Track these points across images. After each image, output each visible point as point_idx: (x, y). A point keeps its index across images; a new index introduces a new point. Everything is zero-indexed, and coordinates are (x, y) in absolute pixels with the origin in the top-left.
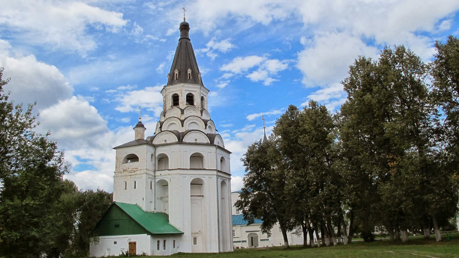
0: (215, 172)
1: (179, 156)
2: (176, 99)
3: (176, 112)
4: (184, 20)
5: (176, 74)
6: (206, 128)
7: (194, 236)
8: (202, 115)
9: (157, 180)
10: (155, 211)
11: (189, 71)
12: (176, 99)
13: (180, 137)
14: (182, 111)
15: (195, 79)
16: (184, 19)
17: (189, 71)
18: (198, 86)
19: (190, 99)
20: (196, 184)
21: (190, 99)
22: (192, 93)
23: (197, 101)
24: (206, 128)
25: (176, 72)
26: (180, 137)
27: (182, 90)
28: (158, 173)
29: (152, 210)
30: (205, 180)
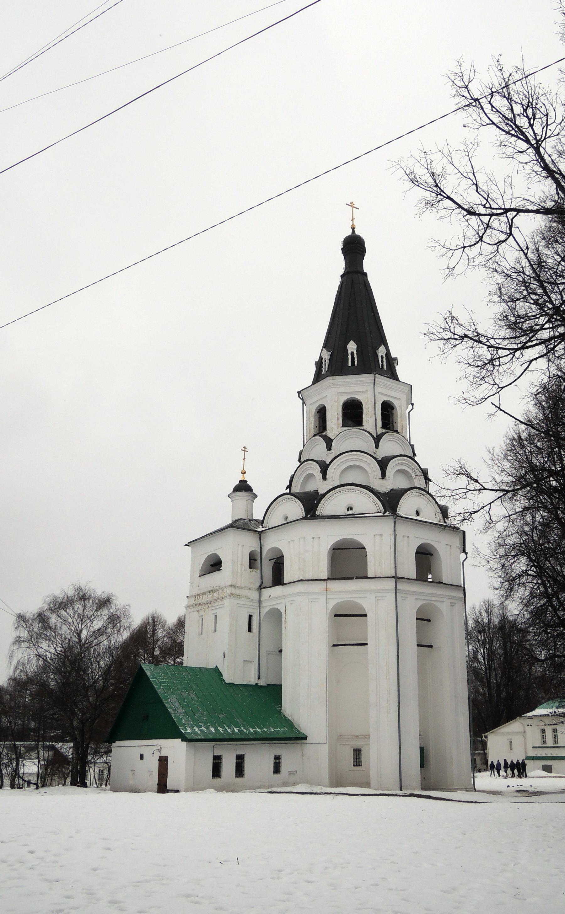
0: (391, 584)
1: (306, 548)
4: (353, 232)
6: (383, 476)
7: (357, 744)
8: (377, 447)
9: (264, 611)
10: (262, 683)
11: (352, 347)
13: (311, 503)
14: (329, 442)
16: (353, 229)
17: (352, 347)
19: (353, 413)
21: (353, 413)
24: (383, 476)
26: (311, 503)
27: (337, 392)
28: (266, 593)
29: (252, 680)
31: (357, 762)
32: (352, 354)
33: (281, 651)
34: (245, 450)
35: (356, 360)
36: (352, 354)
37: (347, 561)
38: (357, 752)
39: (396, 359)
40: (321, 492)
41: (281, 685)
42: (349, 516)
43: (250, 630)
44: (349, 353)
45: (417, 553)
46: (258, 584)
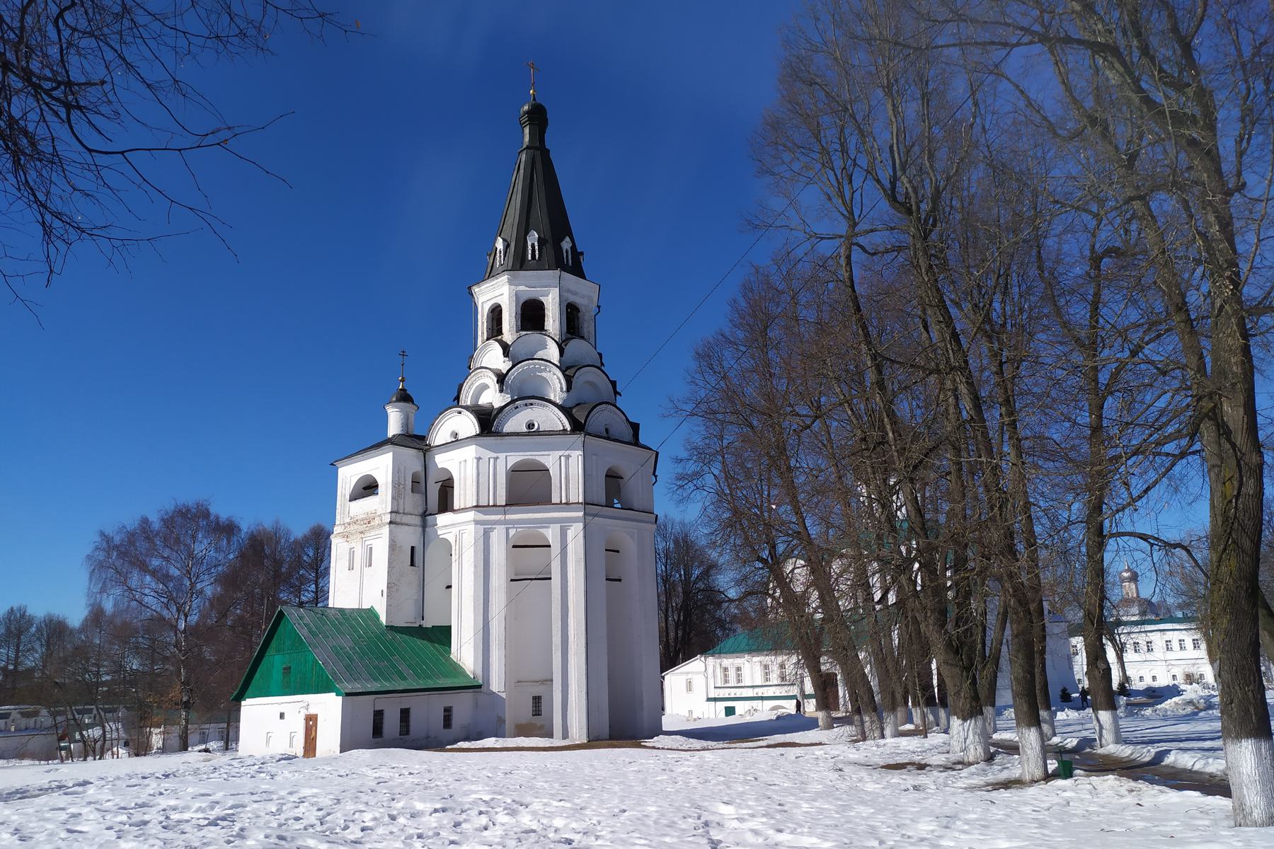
7: (537, 690)
19: (531, 315)
30: (551, 534)
31: (537, 712)
32: (533, 245)
33: (449, 587)
34: (403, 354)
36: (533, 245)
37: (528, 488)
38: (537, 700)
39: (582, 253)
40: (497, 405)
41: (450, 627)
43: (412, 564)
44: (529, 243)
45: (607, 476)
46: (421, 510)
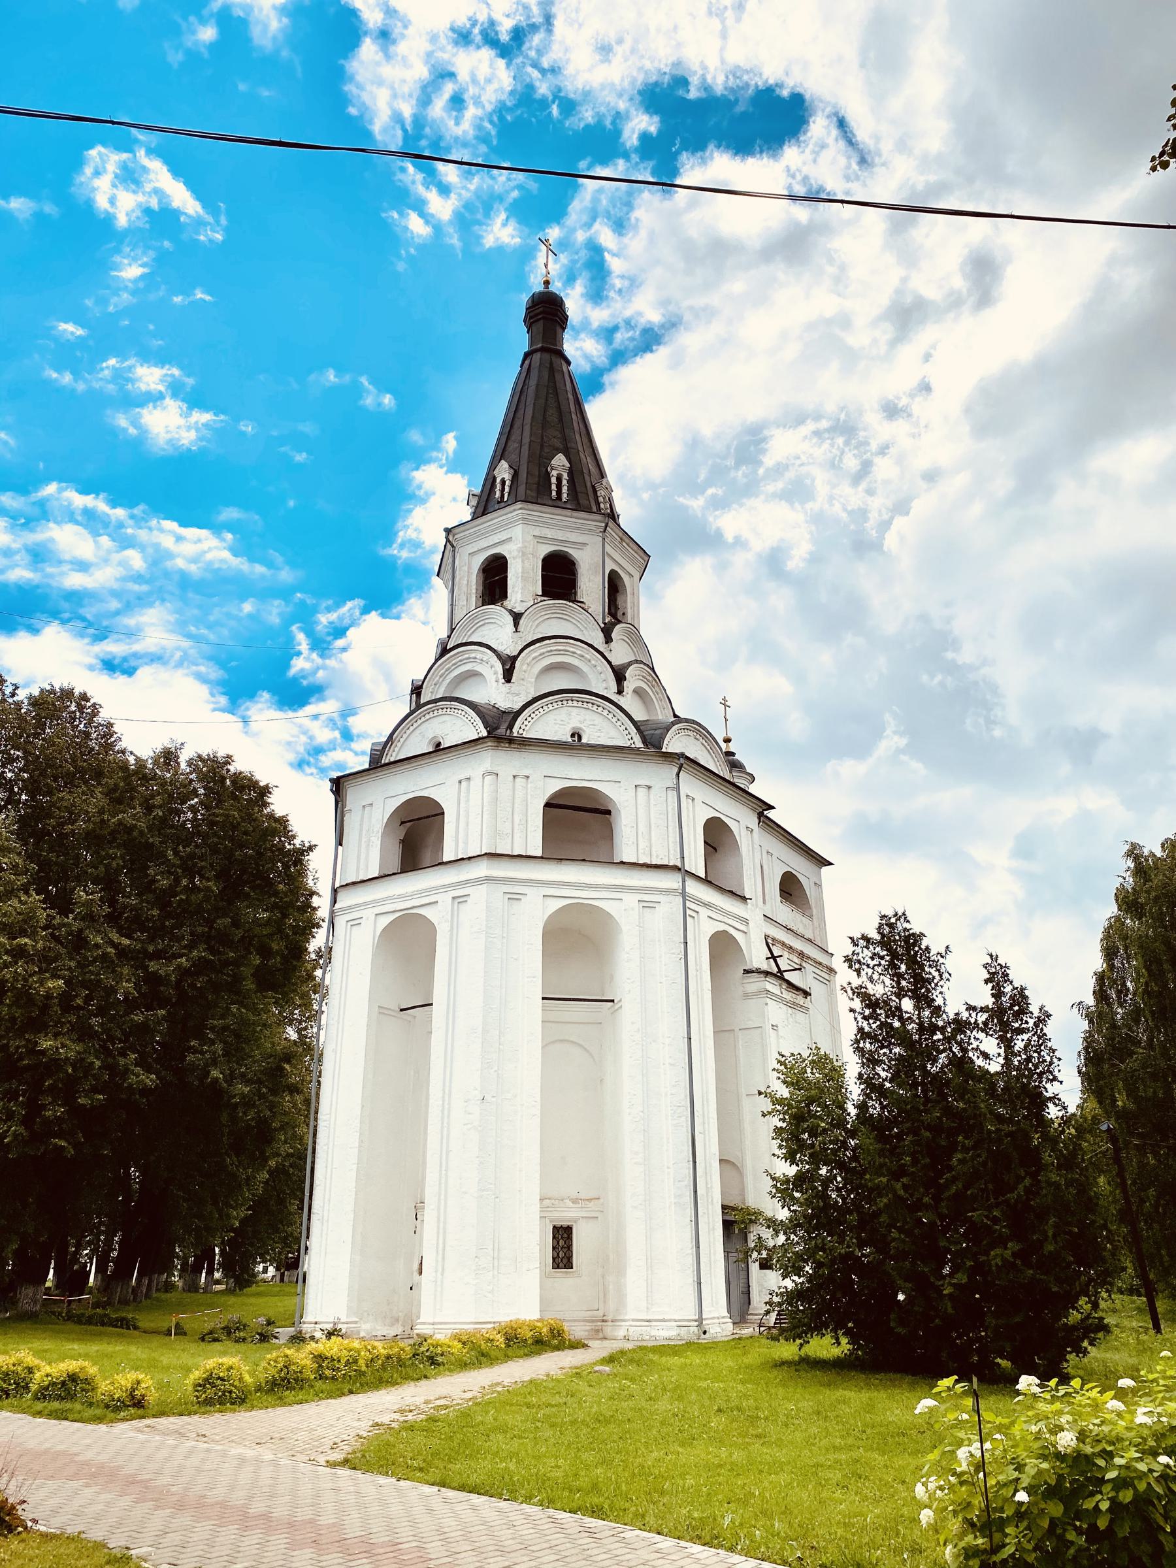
2: (494, 580)
3: (497, 630)
5: (503, 482)
7: (564, 1216)
12: (494, 580)
15: (586, 493)
18: (593, 522)
19: (559, 577)
20: (576, 940)
22: (574, 553)
23: (591, 587)
25: (504, 472)
27: (523, 539)
35: (565, 489)
42: (575, 745)
